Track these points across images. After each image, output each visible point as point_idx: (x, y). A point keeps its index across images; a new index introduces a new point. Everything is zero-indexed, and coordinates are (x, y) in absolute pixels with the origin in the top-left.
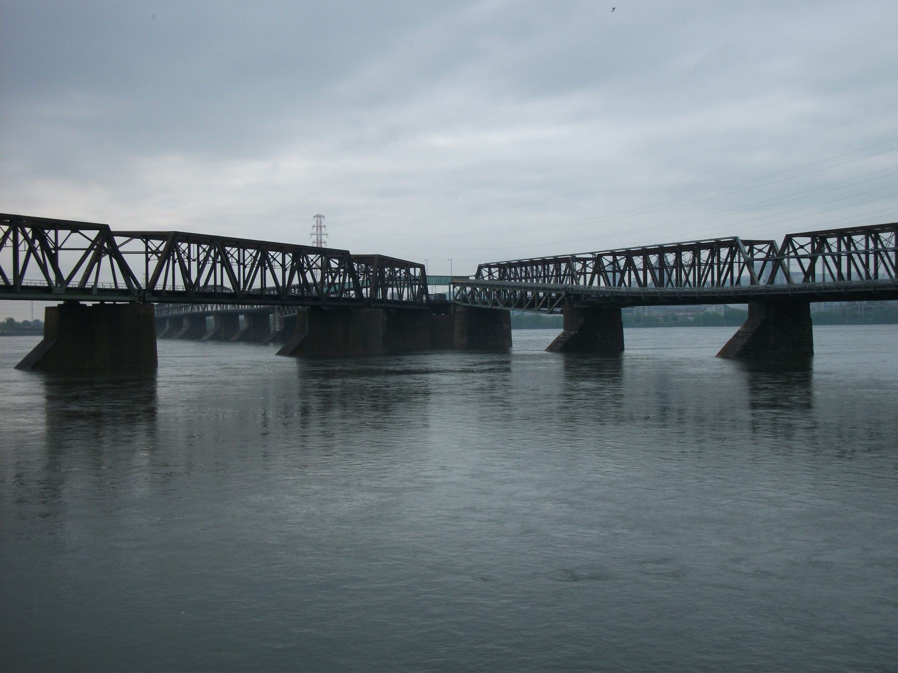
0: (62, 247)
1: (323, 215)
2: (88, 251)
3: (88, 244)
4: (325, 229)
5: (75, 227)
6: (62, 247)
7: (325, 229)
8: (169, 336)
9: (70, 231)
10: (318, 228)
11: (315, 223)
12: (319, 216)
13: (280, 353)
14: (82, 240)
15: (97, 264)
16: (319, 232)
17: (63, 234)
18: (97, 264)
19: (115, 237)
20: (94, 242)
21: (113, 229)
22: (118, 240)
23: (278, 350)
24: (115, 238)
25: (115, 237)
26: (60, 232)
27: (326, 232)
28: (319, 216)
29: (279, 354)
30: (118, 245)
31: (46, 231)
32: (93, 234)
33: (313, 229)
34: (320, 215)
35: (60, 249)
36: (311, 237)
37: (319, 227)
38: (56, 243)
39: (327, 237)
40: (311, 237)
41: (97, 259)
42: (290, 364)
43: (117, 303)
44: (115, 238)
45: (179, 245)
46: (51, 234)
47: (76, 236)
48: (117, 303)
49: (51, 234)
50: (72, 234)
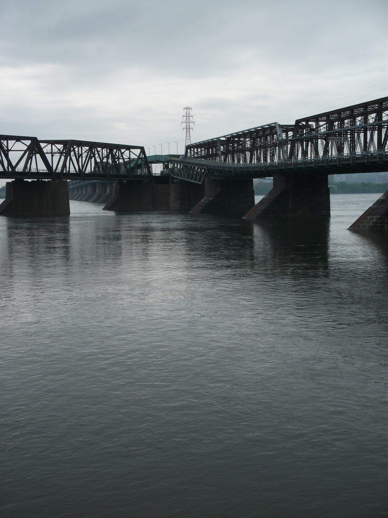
0: (11, 150)
1: (190, 107)
2: (25, 152)
3: (25, 148)
4: (193, 119)
5: (18, 139)
6: (11, 150)
7: (193, 119)
8: (71, 199)
9: (15, 141)
10: (187, 117)
11: (185, 113)
12: (187, 108)
13: (103, 209)
14: (22, 146)
15: (30, 160)
16: (188, 120)
17: (11, 143)
18: (30, 160)
19: (40, 143)
20: (29, 147)
21: (39, 139)
22: (42, 145)
23: (104, 207)
24: (41, 144)
25: (40, 143)
26: (9, 141)
27: (193, 121)
28: (188, 108)
29: (103, 209)
30: (42, 147)
31: (2, 141)
32: (28, 142)
33: (183, 119)
34: (189, 107)
35: (10, 150)
36: (181, 125)
37: (188, 116)
38: (7, 147)
39: (194, 125)
40: (181, 125)
41: (30, 158)
42: (112, 214)
43: (43, 180)
44: (41, 144)
45: (75, 147)
46: (5, 143)
47: (18, 143)
48: (43, 180)
49: (5, 143)
50: (16, 142)
